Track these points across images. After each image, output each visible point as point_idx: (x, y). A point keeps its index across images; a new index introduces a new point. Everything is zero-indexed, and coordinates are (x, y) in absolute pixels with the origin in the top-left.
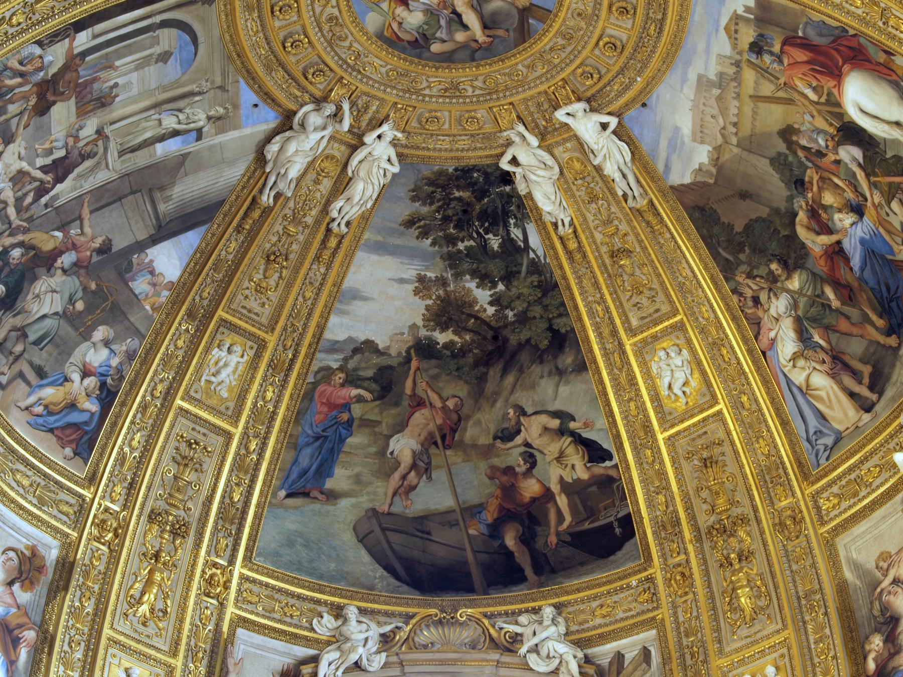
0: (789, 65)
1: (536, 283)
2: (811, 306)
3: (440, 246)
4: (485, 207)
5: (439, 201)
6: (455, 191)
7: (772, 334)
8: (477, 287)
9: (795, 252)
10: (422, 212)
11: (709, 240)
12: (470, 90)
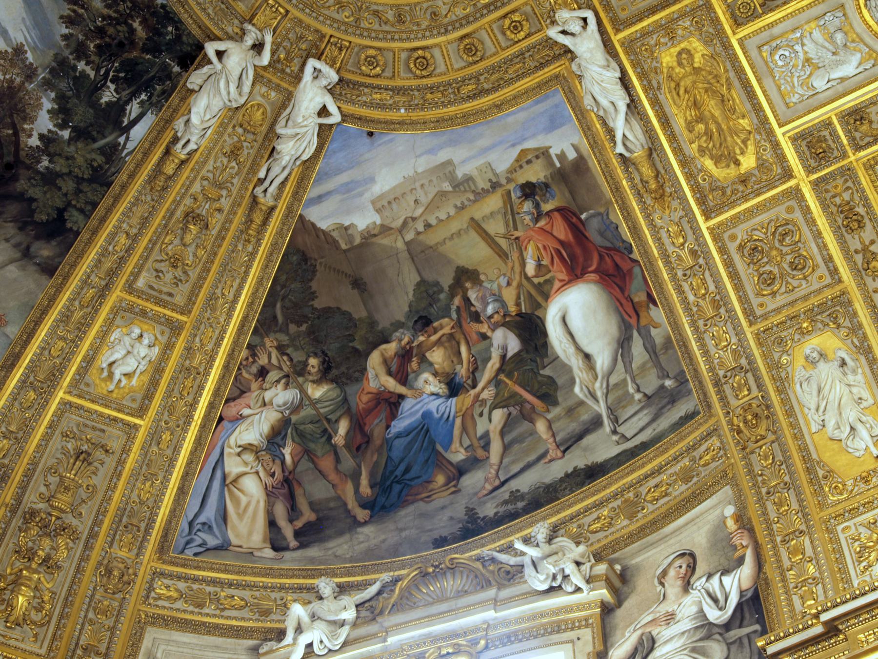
0: (541, 228)
1: (95, 164)
2: (311, 422)
3: (67, 46)
4: (141, 60)
5: (117, 11)
6: (138, 21)
7: (246, 412)
8: (49, 112)
9: (349, 369)
10: (94, 3)
11: (279, 288)
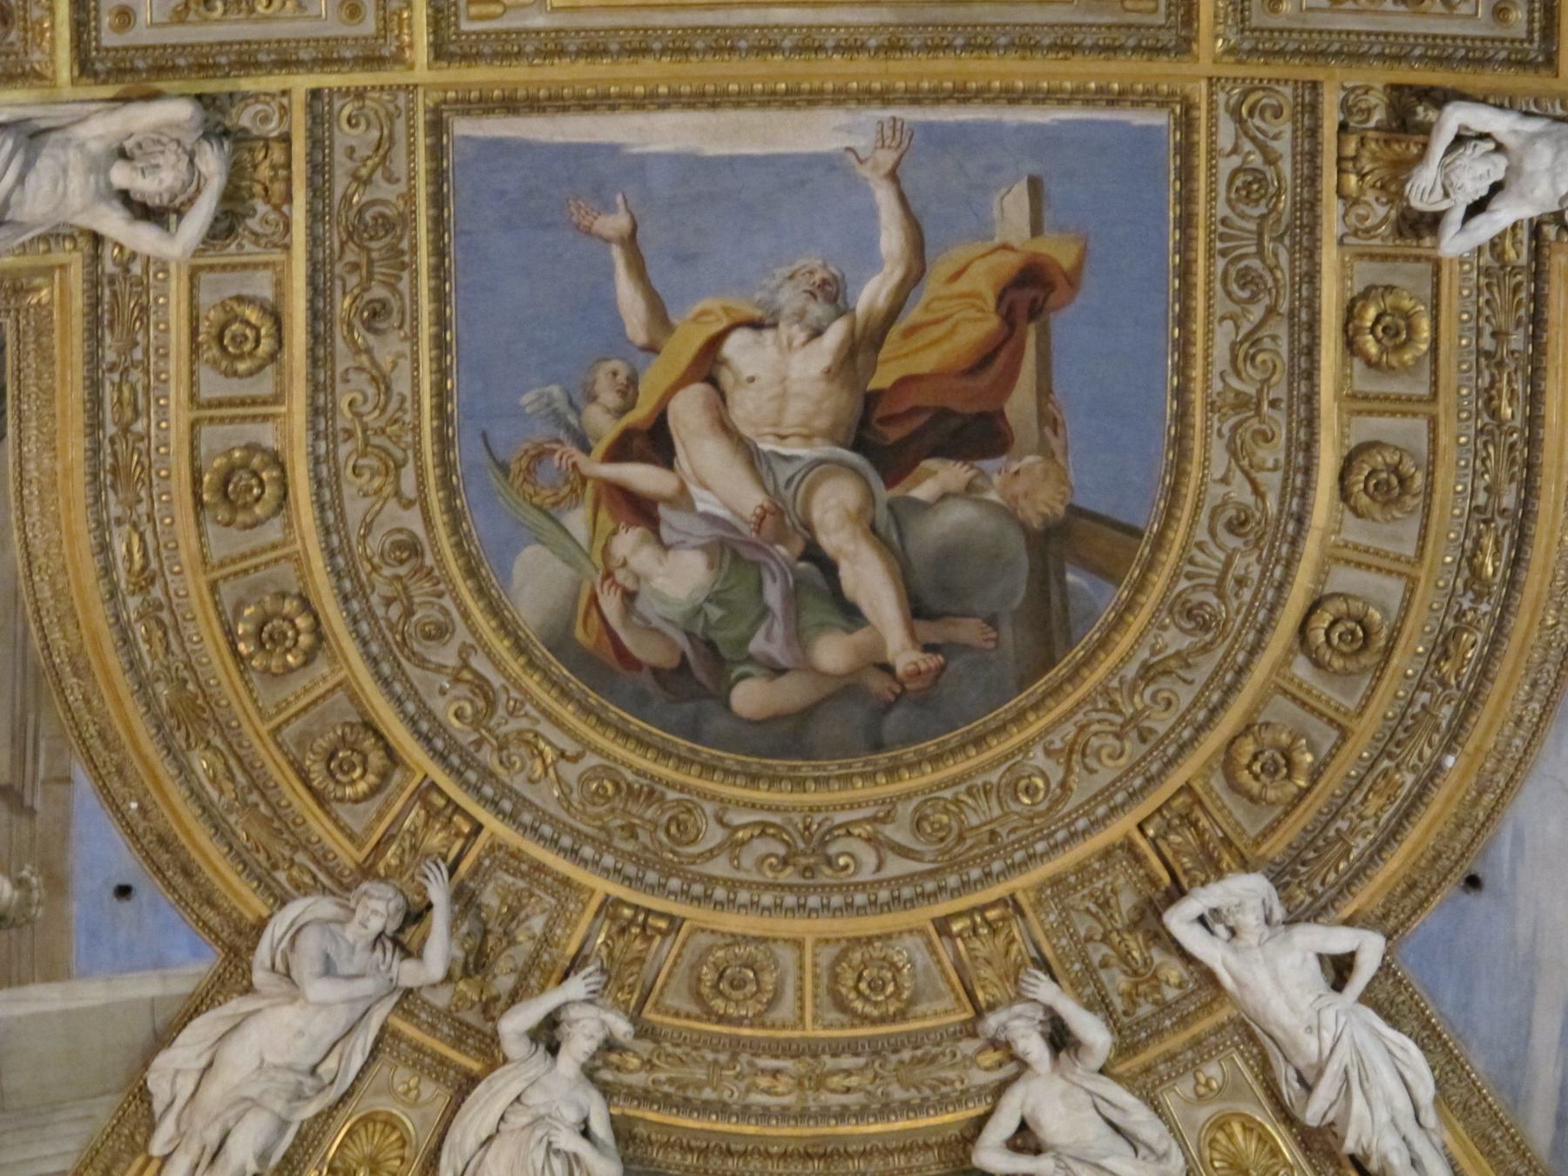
12: (868, 857)
